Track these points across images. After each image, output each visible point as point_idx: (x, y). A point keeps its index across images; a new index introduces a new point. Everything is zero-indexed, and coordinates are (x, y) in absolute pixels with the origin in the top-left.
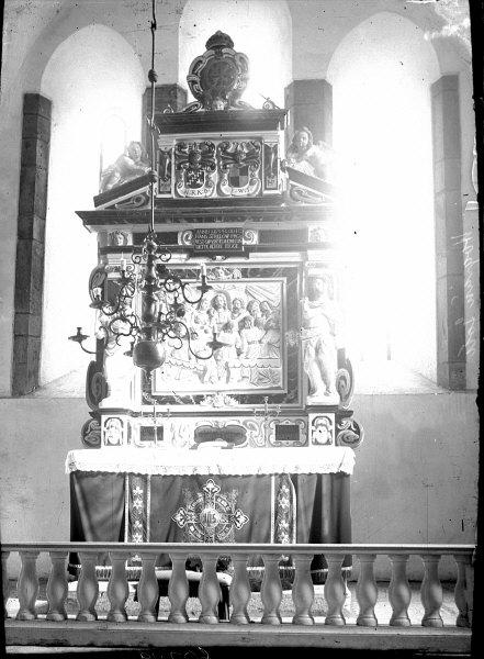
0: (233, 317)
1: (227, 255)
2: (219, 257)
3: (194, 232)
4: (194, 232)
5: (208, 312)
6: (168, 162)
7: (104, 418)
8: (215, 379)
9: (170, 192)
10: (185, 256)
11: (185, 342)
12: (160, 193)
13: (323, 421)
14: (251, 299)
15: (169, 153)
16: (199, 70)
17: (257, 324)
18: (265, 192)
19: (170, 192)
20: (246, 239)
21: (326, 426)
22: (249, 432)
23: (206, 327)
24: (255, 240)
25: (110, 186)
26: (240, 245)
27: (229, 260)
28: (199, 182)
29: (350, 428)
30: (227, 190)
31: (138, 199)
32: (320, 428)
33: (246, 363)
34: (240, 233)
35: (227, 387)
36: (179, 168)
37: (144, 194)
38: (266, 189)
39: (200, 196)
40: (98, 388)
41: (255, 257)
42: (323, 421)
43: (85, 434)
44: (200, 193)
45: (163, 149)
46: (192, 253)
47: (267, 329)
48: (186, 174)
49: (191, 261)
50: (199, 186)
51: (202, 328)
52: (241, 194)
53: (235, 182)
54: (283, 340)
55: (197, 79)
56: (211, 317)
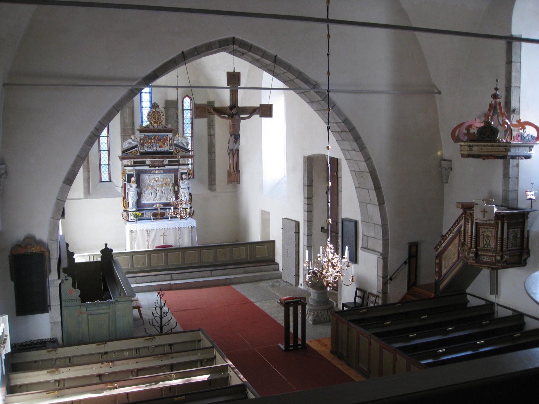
1: (159, 167)
3: (151, 161)
4: (151, 161)
9: (144, 150)
18: (170, 151)
28: (151, 147)
30: (159, 149)
34: (163, 161)
40: (125, 204)
41: (167, 167)
43: (123, 216)
44: (150, 150)
46: (149, 165)
50: (151, 148)
53: (161, 147)
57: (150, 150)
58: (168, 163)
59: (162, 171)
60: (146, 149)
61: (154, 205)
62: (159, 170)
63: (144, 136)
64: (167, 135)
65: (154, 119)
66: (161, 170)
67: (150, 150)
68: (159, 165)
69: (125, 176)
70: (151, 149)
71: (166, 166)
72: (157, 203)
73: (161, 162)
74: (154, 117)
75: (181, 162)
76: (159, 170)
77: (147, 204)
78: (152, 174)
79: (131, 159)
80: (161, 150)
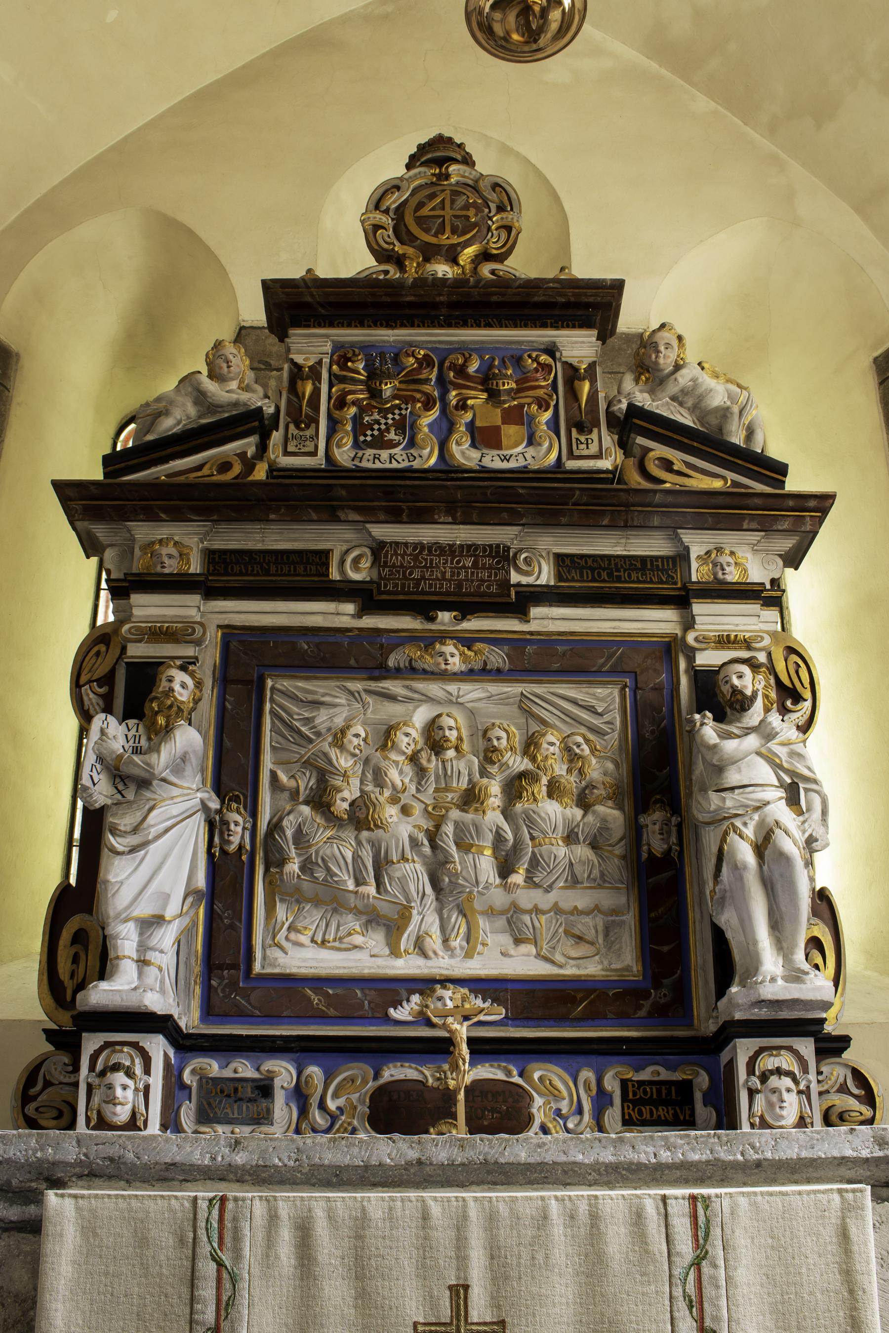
0: (484, 773)
1: (465, 610)
2: (445, 617)
3: (378, 549)
4: (378, 549)
5: (413, 759)
6: (309, 388)
7: (91, 1043)
8: (434, 942)
9: (314, 454)
10: (350, 608)
11: (349, 834)
12: (286, 453)
13: (786, 1061)
14: (534, 727)
15: (315, 373)
16: (393, 201)
17: (554, 790)
18: (571, 465)
19: (314, 454)
20: (518, 570)
21: (790, 1074)
22: (538, 1101)
23: (405, 799)
24: (545, 575)
25: (150, 437)
26: (506, 584)
27: (474, 624)
28: (392, 436)
29: (843, 1089)
31: (225, 467)
32: (774, 1081)
33: (527, 898)
35: (476, 967)
36: (341, 403)
37: (242, 456)
38: (571, 456)
39: (395, 465)
40: (75, 959)
42: (786, 1061)
43: (26, 1098)
45: (299, 359)
47: (584, 802)
48: (357, 420)
49: (370, 622)
50: (391, 445)
51: (394, 800)
52: (505, 465)
54: (635, 832)
55: (387, 221)
56: (421, 772)
57: (376, 458)
58: (559, 577)
59: (497, 657)
60: (344, 455)
61: (397, 1003)
62: (467, 641)
63: (328, 348)
64: (551, 350)
65: (427, 231)
66: (495, 639)
67: (376, 458)
68: (459, 585)
69: (108, 679)
70: (385, 454)
71: (535, 611)
72: (445, 981)
73: (488, 561)
74: (425, 211)
75: (698, 572)
76: (467, 641)
77: (319, 982)
78: (397, 673)
79: (177, 516)
80: (487, 462)
